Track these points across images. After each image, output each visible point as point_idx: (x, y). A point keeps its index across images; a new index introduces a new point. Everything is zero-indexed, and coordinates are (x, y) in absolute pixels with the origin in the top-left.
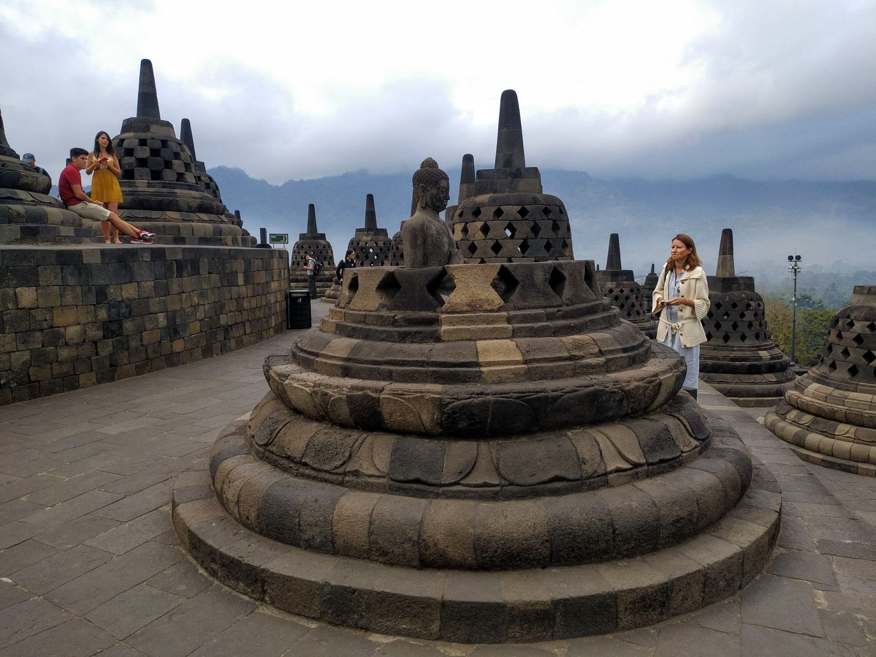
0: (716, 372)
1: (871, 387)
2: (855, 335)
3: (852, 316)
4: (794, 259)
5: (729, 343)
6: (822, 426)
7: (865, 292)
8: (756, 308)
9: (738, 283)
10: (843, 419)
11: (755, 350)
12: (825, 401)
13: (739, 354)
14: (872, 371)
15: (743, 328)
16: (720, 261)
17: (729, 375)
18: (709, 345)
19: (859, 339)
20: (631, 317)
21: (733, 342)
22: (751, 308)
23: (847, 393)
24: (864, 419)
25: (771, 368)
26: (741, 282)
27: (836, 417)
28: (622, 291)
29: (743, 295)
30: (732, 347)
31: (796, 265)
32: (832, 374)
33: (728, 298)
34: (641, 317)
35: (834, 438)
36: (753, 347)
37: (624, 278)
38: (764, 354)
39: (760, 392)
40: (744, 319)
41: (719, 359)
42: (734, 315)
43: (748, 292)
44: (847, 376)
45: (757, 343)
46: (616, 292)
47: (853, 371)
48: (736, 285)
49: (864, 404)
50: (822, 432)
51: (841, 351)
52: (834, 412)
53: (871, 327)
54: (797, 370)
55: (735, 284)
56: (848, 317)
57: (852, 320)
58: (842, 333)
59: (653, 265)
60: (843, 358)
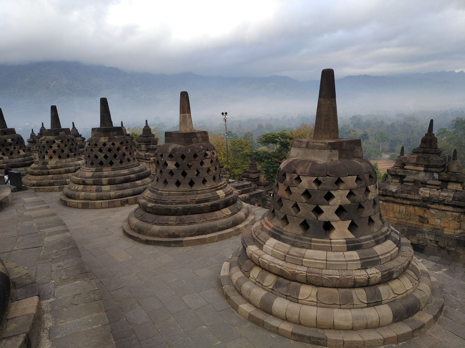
0: (186, 214)
1: (323, 243)
2: (304, 190)
3: (299, 170)
4: (224, 114)
5: (194, 188)
6: (285, 289)
7: (303, 146)
8: (212, 156)
9: (196, 137)
10: (305, 281)
11: (214, 191)
12: (285, 260)
13: (202, 196)
14: (322, 226)
15: (203, 174)
16: (181, 118)
17: (197, 215)
18: (179, 191)
19: (307, 194)
20: (124, 164)
21: (198, 187)
22: (208, 156)
23: (303, 251)
24: (324, 281)
25: (227, 204)
26: (198, 135)
27: (298, 278)
28: (113, 144)
29: (201, 147)
30: (197, 190)
31: (225, 117)
32: (285, 229)
33: (189, 151)
34: (132, 163)
35: (298, 303)
36: (212, 188)
37: (115, 133)
38: (221, 193)
39: (221, 227)
40: (204, 166)
41: (187, 203)
42: (196, 164)
43: (204, 143)
44: (300, 231)
45: (215, 184)
46: (109, 145)
47: (305, 225)
48: (195, 138)
49: (320, 263)
50: (286, 296)
51: (292, 206)
52: (294, 274)
53: (318, 182)
54: (237, 185)
55: (194, 137)
56: (295, 172)
57: (299, 176)
58: (291, 188)
59: (146, 121)
60: (293, 213)
